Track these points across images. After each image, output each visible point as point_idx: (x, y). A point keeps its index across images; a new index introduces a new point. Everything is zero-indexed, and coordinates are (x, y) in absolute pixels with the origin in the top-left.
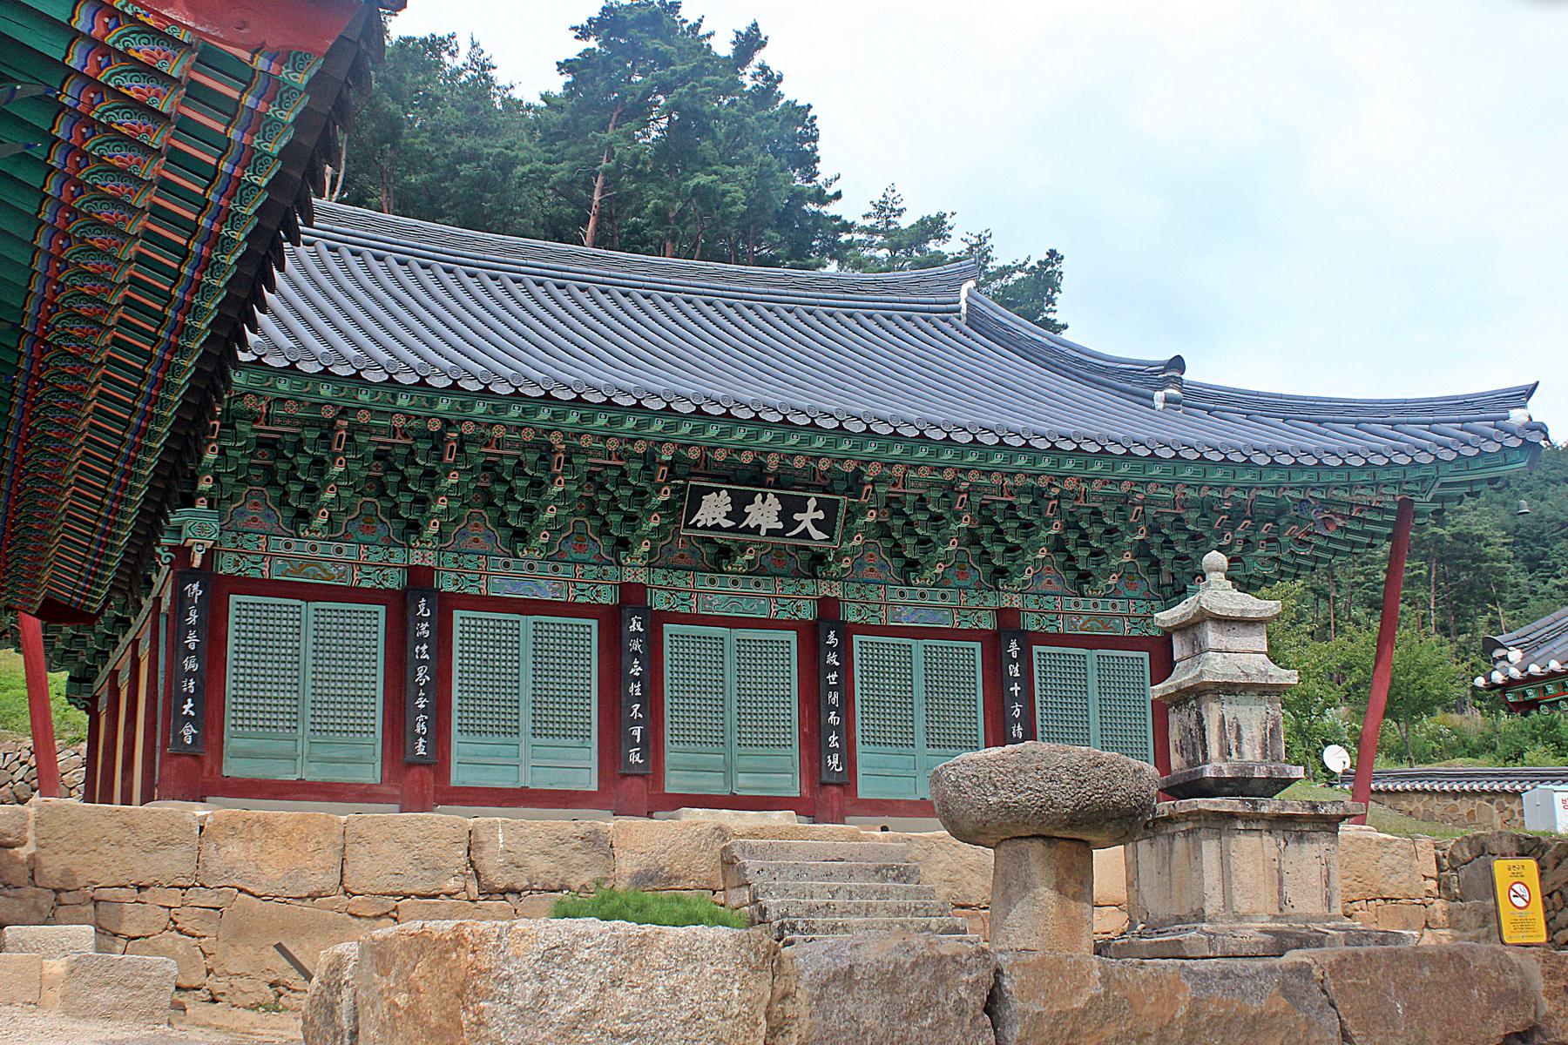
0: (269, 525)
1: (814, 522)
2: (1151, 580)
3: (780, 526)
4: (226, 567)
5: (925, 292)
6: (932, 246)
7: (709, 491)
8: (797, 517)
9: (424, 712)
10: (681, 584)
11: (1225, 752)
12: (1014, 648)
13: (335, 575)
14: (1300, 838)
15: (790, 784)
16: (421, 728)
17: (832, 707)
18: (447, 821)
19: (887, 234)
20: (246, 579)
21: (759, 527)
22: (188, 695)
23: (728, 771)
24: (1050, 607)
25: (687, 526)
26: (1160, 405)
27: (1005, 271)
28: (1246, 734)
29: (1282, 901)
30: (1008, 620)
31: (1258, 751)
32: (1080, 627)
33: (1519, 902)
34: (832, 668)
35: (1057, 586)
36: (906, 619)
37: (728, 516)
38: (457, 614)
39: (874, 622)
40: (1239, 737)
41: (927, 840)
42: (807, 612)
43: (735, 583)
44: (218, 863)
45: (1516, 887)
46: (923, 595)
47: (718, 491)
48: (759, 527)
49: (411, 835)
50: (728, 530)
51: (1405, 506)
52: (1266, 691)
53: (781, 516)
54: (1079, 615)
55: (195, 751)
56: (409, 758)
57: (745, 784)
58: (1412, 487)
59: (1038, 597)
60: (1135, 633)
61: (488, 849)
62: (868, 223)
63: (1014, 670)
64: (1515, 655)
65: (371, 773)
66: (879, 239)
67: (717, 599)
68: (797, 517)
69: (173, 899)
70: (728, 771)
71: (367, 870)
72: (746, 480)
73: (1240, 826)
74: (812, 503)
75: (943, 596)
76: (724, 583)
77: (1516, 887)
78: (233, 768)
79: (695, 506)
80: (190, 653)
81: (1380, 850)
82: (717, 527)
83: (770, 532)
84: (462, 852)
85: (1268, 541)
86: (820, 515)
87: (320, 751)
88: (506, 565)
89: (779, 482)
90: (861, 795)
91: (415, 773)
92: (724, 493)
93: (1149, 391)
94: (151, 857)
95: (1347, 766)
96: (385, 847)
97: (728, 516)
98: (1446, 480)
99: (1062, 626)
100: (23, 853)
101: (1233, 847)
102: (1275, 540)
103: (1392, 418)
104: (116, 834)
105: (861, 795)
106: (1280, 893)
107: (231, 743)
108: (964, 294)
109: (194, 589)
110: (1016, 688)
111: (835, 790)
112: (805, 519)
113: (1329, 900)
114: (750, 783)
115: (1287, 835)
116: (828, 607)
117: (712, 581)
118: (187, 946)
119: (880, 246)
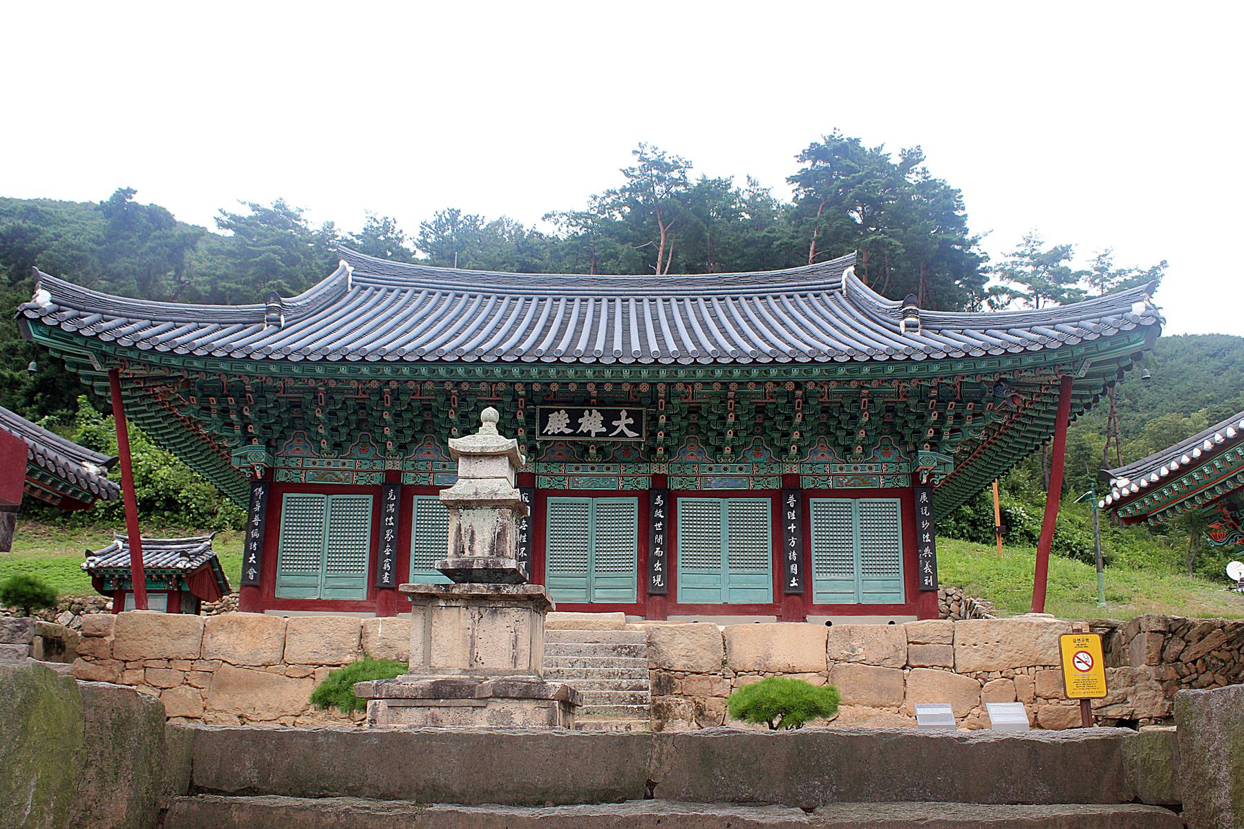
0: (306, 453)
1: (627, 425)
3: (604, 430)
4: (281, 477)
5: (816, 278)
7: (552, 411)
9: (389, 557)
10: (556, 472)
11: (460, 550)
12: (791, 501)
13: (344, 479)
14: (495, 612)
15: (630, 596)
16: (387, 566)
17: (658, 545)
18: (274, 616)
20: (292, 484)
21: (589, 432)
22: (252, 551)
23: (588, 588)
25: (541, 434)
26: (902, 329)
28: (478, 537)
30: (791, 483)
31: (487, 550)
32: (845, 483)
33: (1082, 666)
34: (659, 520)
37: (568, 426)
38: (416, 498)
39: (692, 488)
40: (472, 540)
41: (671, 629)
42: (644, 484)
43: (593, 469)
44: (212, 646)
45: (1080, 655)
47: (559, 411)
48: (589, 432)
49: (325, 628)
50: (569, 435)
52: (496, 504)
53: (604, 424)
54: (845, 475)
55: (257, 583)
56: (378, 584)
57: (600, 596)
58: (1067, 367)
59: (821, 467)
60: (889, 486)
64: (1122, 482)
65: (361, 595)
69: (186, 666)
70: (588, 588)
73: (442, 603)
74: (624, 414)
75: (741, 469)
77: (1080, 655)
78: (282, 593)
79: (544, 422)
80: (255, 527)
82: (561, 434)
83: (598, 434)
84: (355, 639)
85: (974, 415)
86: (631, 421)
88: (444, 466)
89: (601, 402)
90: (679, 602)
93: (896, 321)
97: (568, 426)
98: (1095, 359)
100: (108, 639)
102: (981, 414)
103: (1054, 320)
104: (158, 629)
105: (679, 602)
106: (471, 653)
107: (281, 579)
108: (845, 275)
110: (793, 527)
111: (658, 598)
112: (621, 424)
113: (515, 659)
115: (482, 610)
116: (659, 482)
118: (193, 695)
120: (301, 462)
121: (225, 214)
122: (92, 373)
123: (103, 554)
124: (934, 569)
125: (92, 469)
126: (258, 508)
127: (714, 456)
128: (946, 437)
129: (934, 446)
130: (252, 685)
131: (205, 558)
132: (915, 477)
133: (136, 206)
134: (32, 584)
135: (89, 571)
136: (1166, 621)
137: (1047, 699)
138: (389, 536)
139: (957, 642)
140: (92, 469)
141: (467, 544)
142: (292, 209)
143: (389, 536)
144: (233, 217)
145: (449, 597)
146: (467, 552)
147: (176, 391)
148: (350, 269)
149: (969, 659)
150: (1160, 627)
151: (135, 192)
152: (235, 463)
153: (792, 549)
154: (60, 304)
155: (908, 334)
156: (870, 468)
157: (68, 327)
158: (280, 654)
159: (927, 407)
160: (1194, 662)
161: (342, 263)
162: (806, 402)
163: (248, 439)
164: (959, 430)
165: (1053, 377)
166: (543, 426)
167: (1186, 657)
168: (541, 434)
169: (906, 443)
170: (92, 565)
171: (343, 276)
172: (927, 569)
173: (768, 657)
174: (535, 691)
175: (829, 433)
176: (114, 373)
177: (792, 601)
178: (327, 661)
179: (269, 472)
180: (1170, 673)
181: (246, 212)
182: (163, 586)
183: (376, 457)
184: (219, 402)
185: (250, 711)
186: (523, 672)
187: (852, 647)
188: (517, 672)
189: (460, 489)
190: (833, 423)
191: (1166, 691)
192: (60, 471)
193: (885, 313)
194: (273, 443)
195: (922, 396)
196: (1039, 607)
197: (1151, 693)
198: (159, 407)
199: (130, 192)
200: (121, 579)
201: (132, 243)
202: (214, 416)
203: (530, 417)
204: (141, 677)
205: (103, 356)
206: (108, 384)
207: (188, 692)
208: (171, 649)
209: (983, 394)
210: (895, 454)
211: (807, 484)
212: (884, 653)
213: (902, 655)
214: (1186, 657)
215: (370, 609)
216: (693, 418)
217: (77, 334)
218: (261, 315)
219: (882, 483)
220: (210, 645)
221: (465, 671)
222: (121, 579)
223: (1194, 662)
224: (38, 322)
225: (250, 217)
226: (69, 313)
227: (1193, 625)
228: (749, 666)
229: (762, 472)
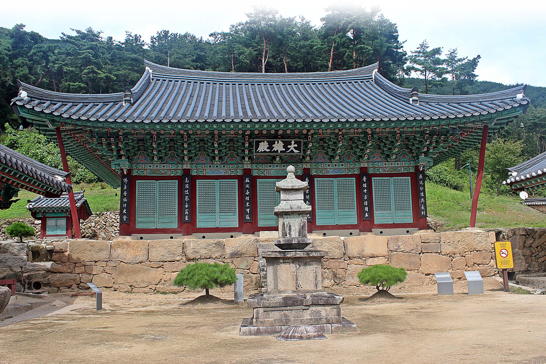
1: (294, 148)
2: (410, 155)
3: (284, 150)
4: (135, 173)
5: (362, 74)
6: (437, 56)
7: (261, 142)
9: (187, 208)
10: (261, 168)
12: (365, 179)
13: (163, 173)
14: (306, 264)
16: (187, 213)
19: (424, 53)
20: (140, 176)
22: (125, 208)
24: (377, 166)
27: (460, 60)
28: (293, 228)
30: (364, 171)
31: (297, 234)
33: (504, 255)
35: (379, 159)
37: (268, 148)
38: (197, 181)
39: (321, 174)
40: (290, 229)
43: (277, 166)
44: (115, 254)
45: (503, 251)
47: (264, 141)
49: (167, 245)
50: (268, 152)
51: (486, 127)
52: (300, 213)
53: (284, 147)
54: (387, 167)
55: (127, 222)
56: (183, 221)
58: (487, 122)
60: (406, 171)
61: (188, 248)
62: (418, 50)
63: (365, 185)
64: (515, 174)
65: (175, 226)
66: (421, 54)
69: (104, 264)
72: (272, 138)
73: (281, 261)
74: (293, 142)
75: (342, 165)
77: (503, 251)
78: (139, 226)
80: (125, 197)
81: (475, 236)
82: (265, 152)
83: (281, 152)
84: (181, 249)
85: (444, 141)
86: (296, 145)
87: (161, 220)
88: (210, 166)
89: (282, 137)
90: (317, 224)
91: (185, 225)
92: (266, 142)
95: (527, 197)
97: (268, 148)
100: (66, 254)
101: (278, 268)
102: (447, 141)
103: (481, 100)
104: (89, 248)
105: (317, 224)
106: (296, 283)
107: (138, 219)
108: (374, 73)
109: (126, 180)
110: (365, 191)
112: (292, 147)
113: (316, 285)
115: (300, 263)
117: (270, 166)
118: (108, 277)
119: (422, 56)
120: (144, 168)
121: (64, 35)
122: (48, 128)
123: (35, 201)
124: (426, 207)
125: (60, 179)
126: (125, 188)
127: (330, 159)
128: (431, 151)
129: (426, 154)
130: (135, 272)
131: (82, 201)
132: (417, 168)
133: (26, 33)
134: (23, 227)
135: (30, 209)
136: (526, 230)
137: (478, 265)
138: (187, 199)
139: (442, 243)
140: (60, 179)
141: (288, 232)
142: (95, 32)
143: (187, 199)
144: (69, 37)
145: (286, 260)
146: (288, 234)
147: (86, 137)
148: (151, 71)
149: (447, 249)
150: (524, 233)
151: (24, 26)
152: (113, 167)
153: (366, 200)
154: (32, 97)
155: (414, 104)
156: (398, 164)
157: (37, 109)
158: (147, 257)
159: (424, 138)
160: (537, 247)
161: (147, 68)
162: (372, 136)
163: (120, 157)
164: (436, 147)
165: (480, 125)
166: (257, 149)
167: (534, 245)
168: (256, 152)
169: (413, 153)
170: (31, 206)
171: (148, 75)
172: (423, 208)
173: (363, 251)
174: (331, 301)
175: (380, 148)
176: (58, 129)
177: (366, 224)
178: (169, 259)
179: (129, 171)
180: (528, 252)
181: (74, 34)
182: (64, 215)
183: (178, 163)
184: (106, 140)
185: (135, 283)
186: (321, 291)
187: (398, 245)
188: (318, 291)
189: (283, 206)
190: (382, 144)
191: (526, 260)
192: (39, 177)
193: (400, 94)
194: (130, 158)
195: (423, 133)
196: (473, 225)
197: (520, 261)
198: (76, 142)
199: (22, 26)
200: (45, 212)
201: (25, 51)
202: (104, 147)
203: (251, 144)
204: (83, 270)
205: (53, 121)
206: (55, 133)
207: (106, 276)
208: (96, 257)
209: (448, 132)
210: (408, 157)
211: (371, 171)
212: (412, 248)
213: (419, 248)
214: (534, 245)
215: (180, 232)
216: (321, 143)
217: (42, 112)
218: (121, 97)
219: (402, 171)
220: (114, 254)
221: (294, 292)
222: (45, 212)
223: (537, 247)
224: (23, 107)
225: (76, 36)
226: (37, 101)
227: (537, 232)
228: (355, 255)
229: (351, 167)
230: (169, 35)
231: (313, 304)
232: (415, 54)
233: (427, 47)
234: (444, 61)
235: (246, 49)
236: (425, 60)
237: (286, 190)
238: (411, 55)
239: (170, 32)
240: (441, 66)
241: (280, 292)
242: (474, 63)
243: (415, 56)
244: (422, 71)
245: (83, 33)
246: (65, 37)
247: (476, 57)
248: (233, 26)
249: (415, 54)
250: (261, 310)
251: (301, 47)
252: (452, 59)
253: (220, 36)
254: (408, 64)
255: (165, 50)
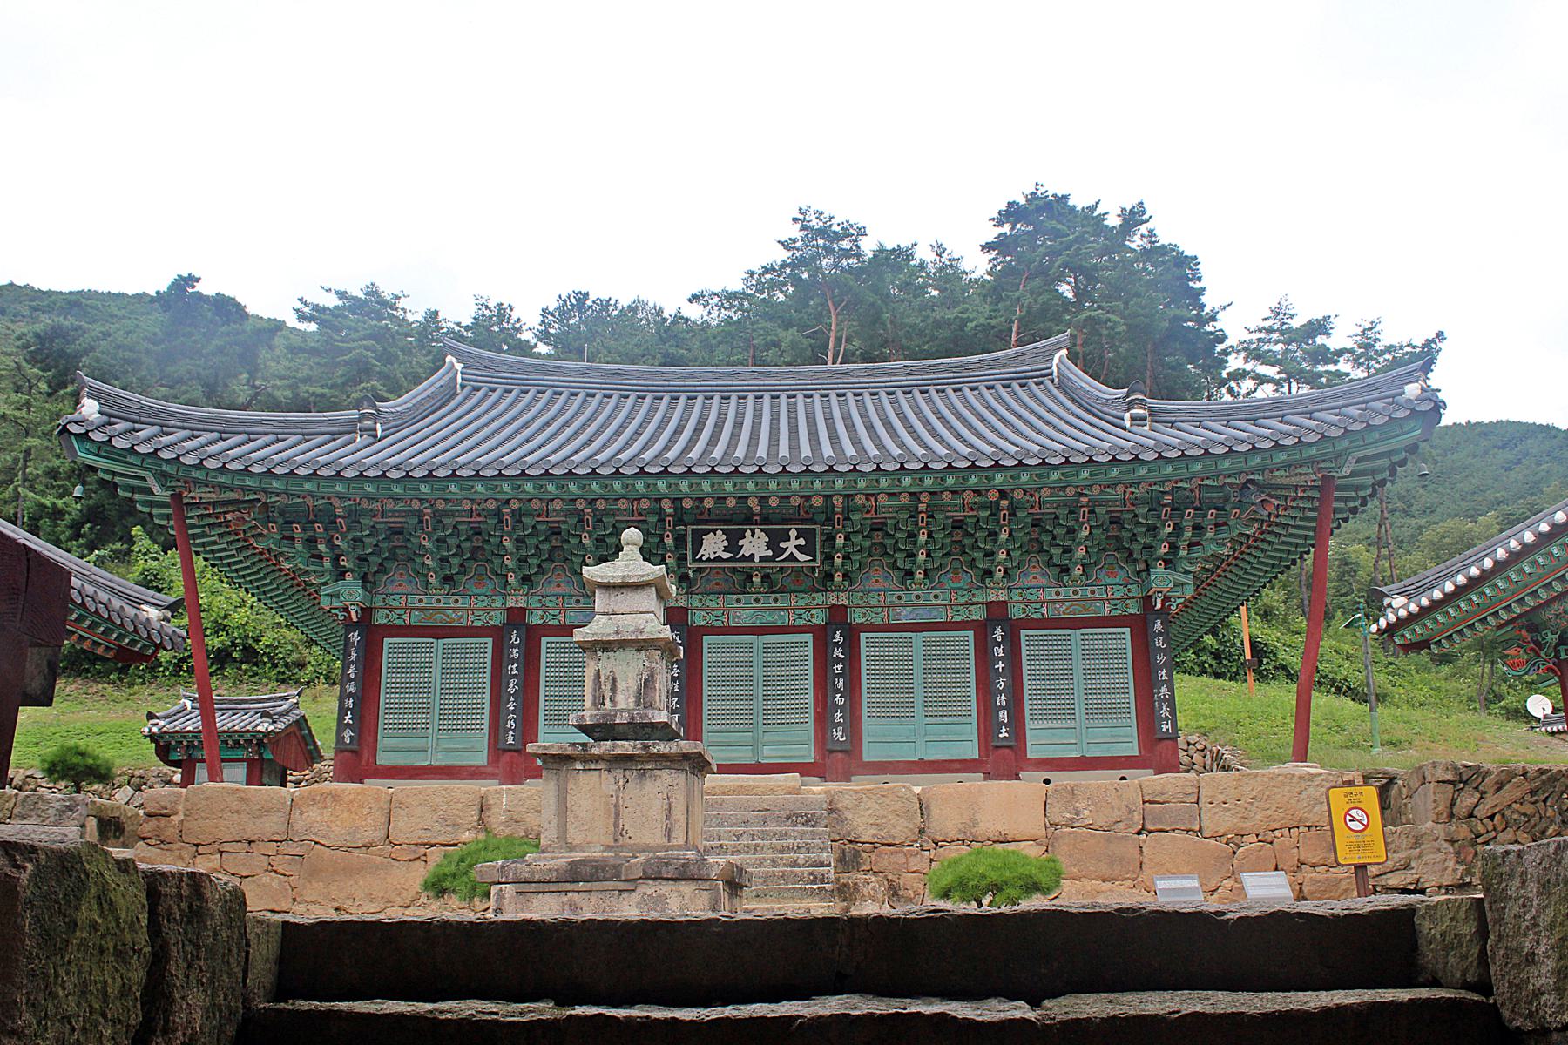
0: (410, 588)
2: (1129, 568)
3: (770, 553)
4: (380, 619)
5: (1023, 364)
7: (707, 532)
8: (782, 545)
9: (513, 712)
10: (713, 605)
11: (599, 701)
13: (455, 619)
14: (643, 774)
15: (806, 753)
16: (511, 724)
17: (838, 691)
18: (374, 786)
20: (394, 626)
21: (752, 555)
23: (754, 745)
24: (1033, 598)
25: (694, 560)
26: (1128, 424)
28: (621, 685)
29: (618, 831)
30: (997, 612)
31: (632, 700)
32: (1063, 611)
34: (838, 660)
35: (1042, 580)
36: (905, 616)
37: (726, 549)
38: (544, 640)
40: (614, 689)
41: (856, 792)
42: (820, 618)
43: (757, 600)
46: (918, 597)
48: (752, 555)
49: (438, 800)
51: (1327, 479)
52: (641, 645)
53: (769, 546)
54: (1063, 601)
55: (355, 747)
56: (501, 746)
57: (769, 755)
59: (1032, 591)
60: (1115, 613)
61: (494, 810)
63: (999, 651)
64: (1398, 601)
65: (480, 759)
67: (744, 614)
68: (782, 545)
70: (754, 745)
71: (405, 827)
72: (736, 522)
73: (579, 766)
74: (793, 533)
75: (936, 597)
76: (748, 601)
78: (384, 759)
79: (698, 544)
81: (1303, 784)
82: (719, 559)
83: (762, 559)
84: (475, 812)
85: (1217, 525)
86: (802, 542)
87: (444, 745)
89: (765, 520)
90: (866, 758)
91: (506, 757)
92: (719, 532)
93: (1119, 414)
94: (258, 822)
95: (1549, 711)
96: (418, 811)
97: (726, 549)
98: (1362, 454)
99: (1047, 612)
100: (176, 819)
101: (571, 785)
102: (1225, 524)
103: (1310, 407)
104: (235, 805)
105: (866, 758)
106: (616, 825)
107: (383, 742)
109: (355, 636)
110: (1001, 665)
111: (840, 755)
112: (791, 545)
113: (669, 832)
114: (774, 754)
115: (628, 773)
116: (838, 614)
117: (738, 601)
120: (404, 600)
122: (149, 497)
124: (1173, 712)
125: (152, 613)
126: (353, 657)
127: (903, 583)
128: (1183, 553)
129: (1169, 563)
130: (351, 871)
131: (291, 718)
132: (1147, 600)
134: (83, 754)
135: (152, 737)
136: (1456, 768)
137: (1314, 866)
138: (512, 686)
139: (1203, 800)
140: (152, 613)
141: (608, 694)
143: (512, 686)
145: (588, 759)
146: (608, 702)
147: (251, 518)
148: (459, 366)
149: (1217, 820)
150: (1449, 776)
152: (325, 602)
153: (1000, 692)
154: (110, 416)
155: (1134, 429)
156: (1093, 592)
157: (120, 443)
158: (384, 832)
159: (1159, 517)
160: (1491, 818)
161: (449, 359)
162: (1012, 514)
163: (341, 574)
164: (1199, 544)
165: (1310, 476)
166: (696, 551)
167: (1481, 812)
168: (694, 560)
169: (1135, 561)
170: (155, 730)
171: (451, 375)
172: (1165, 712)
173: (975, 823)
175: (1041, 551)
176: (177, 497)
177: (1002, 756)
178: (441, 839)
179: (367, 612)
180: (1463, 832)
182: (241, 754)
183: (495, 592)
184: (304, 530)
185: (350, 902)
186: (679, 848)
187: (1076, 809)
188: (672, 848)
189: (599, 628)
190: (1046, 539)
191: (1458, 853)
192: (114, 616)
193: (1106, 405)
194: (371, 578)
195: (1154, 504)
196: (1301, 755)
197: (1440, 856)
200: (190, 746)
202: (299, 546)
203: (680, 540)
204: (216, 864)
205: (163, 477)
206: (170, 511)
207: (274, 881)
208: (252, 829)
209: (1226, 499)
210: (1122, 574)
211: (1017, 612)
212: (1115, 815)
213: (1137, 817)
214: (1481, 812)
215: (492, 776)
216: (878, 537)
217: (131, 450)
218: (353, 423)
219: (1107, 610)
220: (299, 823)
221: (608, 848)
222: (190, 746)
223: (1491, 818)
224: (84, 437)
226: (122, 426)
227: (1489, 773)
228: (952, 835)
229: (962, 600)
230: (589, 303)
231: (646, 877)
232: (1258, 335)
233: (1292, 316)
234: (1340, 353)
235: (782, 333)
236: (1286, 352)
237: (608, 587)
238: (1247, 337)
239: (592, 297)
240: (1331, 368)
241: (571, 848)
242: (1425, 357)
243: (1259, 340)
244: (1277, 383)
245: (355, 298)
246: (307, 310)
247: (1432, 336)
248: (752, 274)
249: (1258, 335)
250: (509, 889)
251: (938, 324)
252: (1366, 348)
253: (716, 299)
254: (1235, 363)
255: (577, 344)
